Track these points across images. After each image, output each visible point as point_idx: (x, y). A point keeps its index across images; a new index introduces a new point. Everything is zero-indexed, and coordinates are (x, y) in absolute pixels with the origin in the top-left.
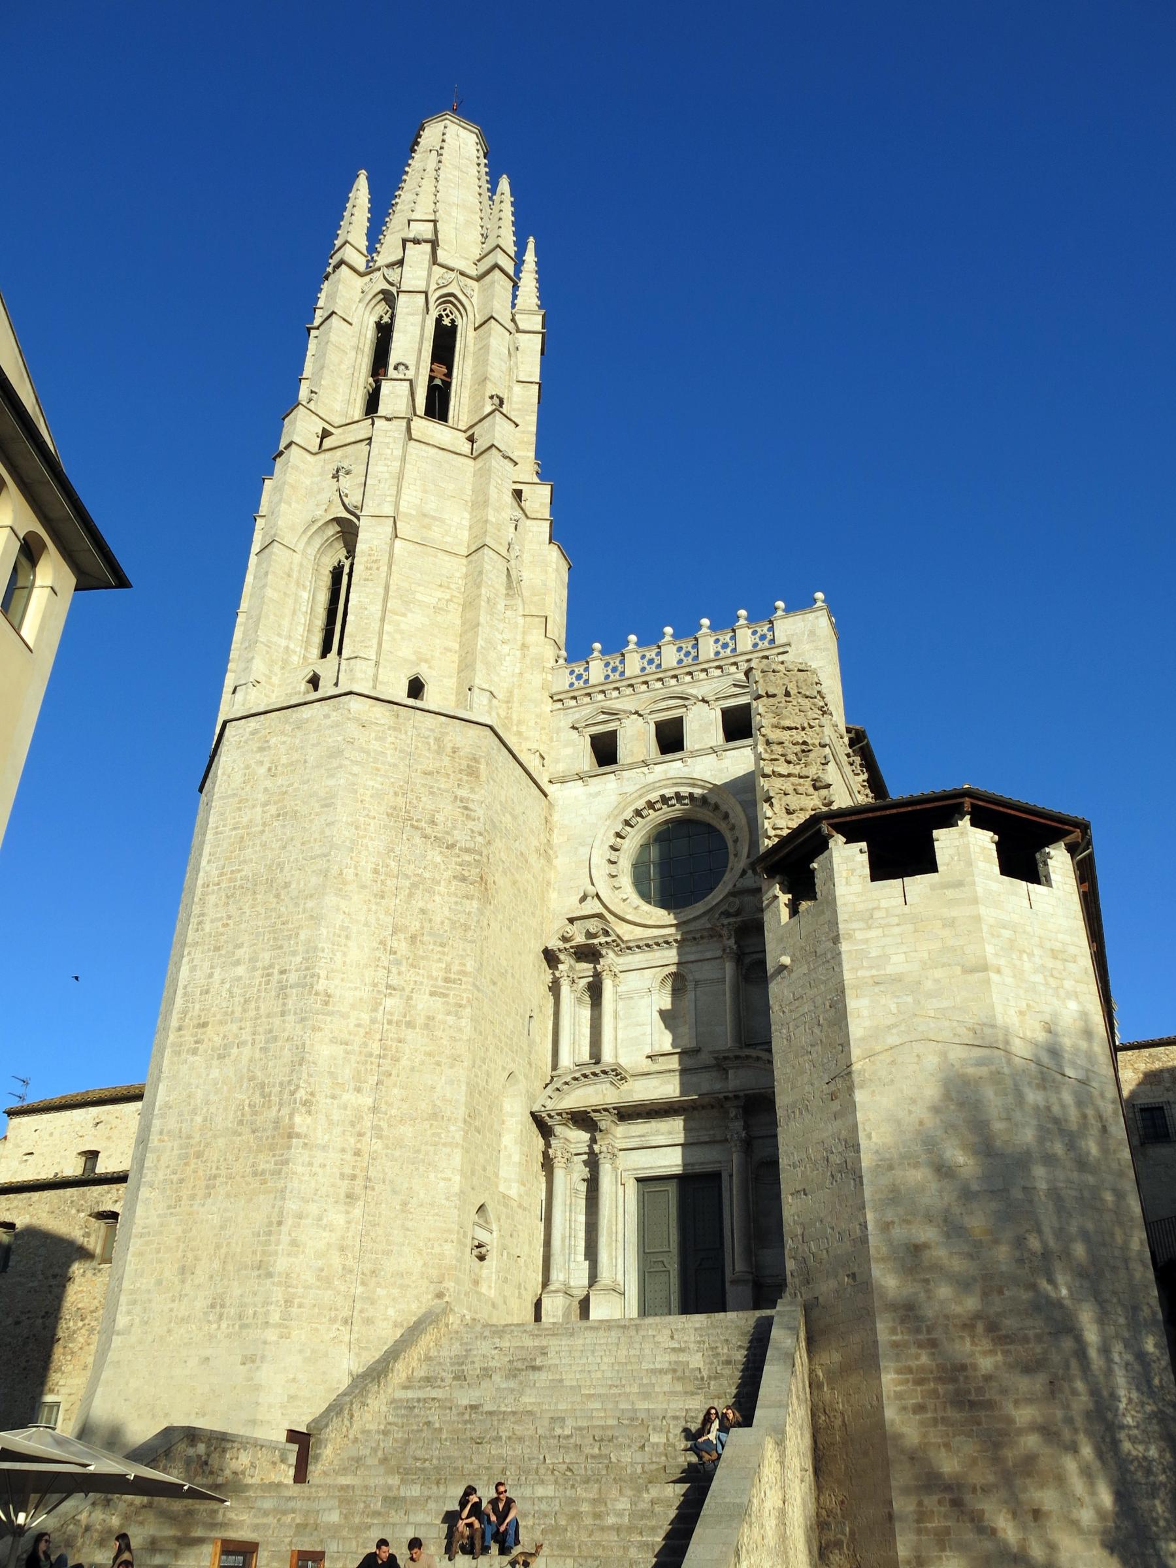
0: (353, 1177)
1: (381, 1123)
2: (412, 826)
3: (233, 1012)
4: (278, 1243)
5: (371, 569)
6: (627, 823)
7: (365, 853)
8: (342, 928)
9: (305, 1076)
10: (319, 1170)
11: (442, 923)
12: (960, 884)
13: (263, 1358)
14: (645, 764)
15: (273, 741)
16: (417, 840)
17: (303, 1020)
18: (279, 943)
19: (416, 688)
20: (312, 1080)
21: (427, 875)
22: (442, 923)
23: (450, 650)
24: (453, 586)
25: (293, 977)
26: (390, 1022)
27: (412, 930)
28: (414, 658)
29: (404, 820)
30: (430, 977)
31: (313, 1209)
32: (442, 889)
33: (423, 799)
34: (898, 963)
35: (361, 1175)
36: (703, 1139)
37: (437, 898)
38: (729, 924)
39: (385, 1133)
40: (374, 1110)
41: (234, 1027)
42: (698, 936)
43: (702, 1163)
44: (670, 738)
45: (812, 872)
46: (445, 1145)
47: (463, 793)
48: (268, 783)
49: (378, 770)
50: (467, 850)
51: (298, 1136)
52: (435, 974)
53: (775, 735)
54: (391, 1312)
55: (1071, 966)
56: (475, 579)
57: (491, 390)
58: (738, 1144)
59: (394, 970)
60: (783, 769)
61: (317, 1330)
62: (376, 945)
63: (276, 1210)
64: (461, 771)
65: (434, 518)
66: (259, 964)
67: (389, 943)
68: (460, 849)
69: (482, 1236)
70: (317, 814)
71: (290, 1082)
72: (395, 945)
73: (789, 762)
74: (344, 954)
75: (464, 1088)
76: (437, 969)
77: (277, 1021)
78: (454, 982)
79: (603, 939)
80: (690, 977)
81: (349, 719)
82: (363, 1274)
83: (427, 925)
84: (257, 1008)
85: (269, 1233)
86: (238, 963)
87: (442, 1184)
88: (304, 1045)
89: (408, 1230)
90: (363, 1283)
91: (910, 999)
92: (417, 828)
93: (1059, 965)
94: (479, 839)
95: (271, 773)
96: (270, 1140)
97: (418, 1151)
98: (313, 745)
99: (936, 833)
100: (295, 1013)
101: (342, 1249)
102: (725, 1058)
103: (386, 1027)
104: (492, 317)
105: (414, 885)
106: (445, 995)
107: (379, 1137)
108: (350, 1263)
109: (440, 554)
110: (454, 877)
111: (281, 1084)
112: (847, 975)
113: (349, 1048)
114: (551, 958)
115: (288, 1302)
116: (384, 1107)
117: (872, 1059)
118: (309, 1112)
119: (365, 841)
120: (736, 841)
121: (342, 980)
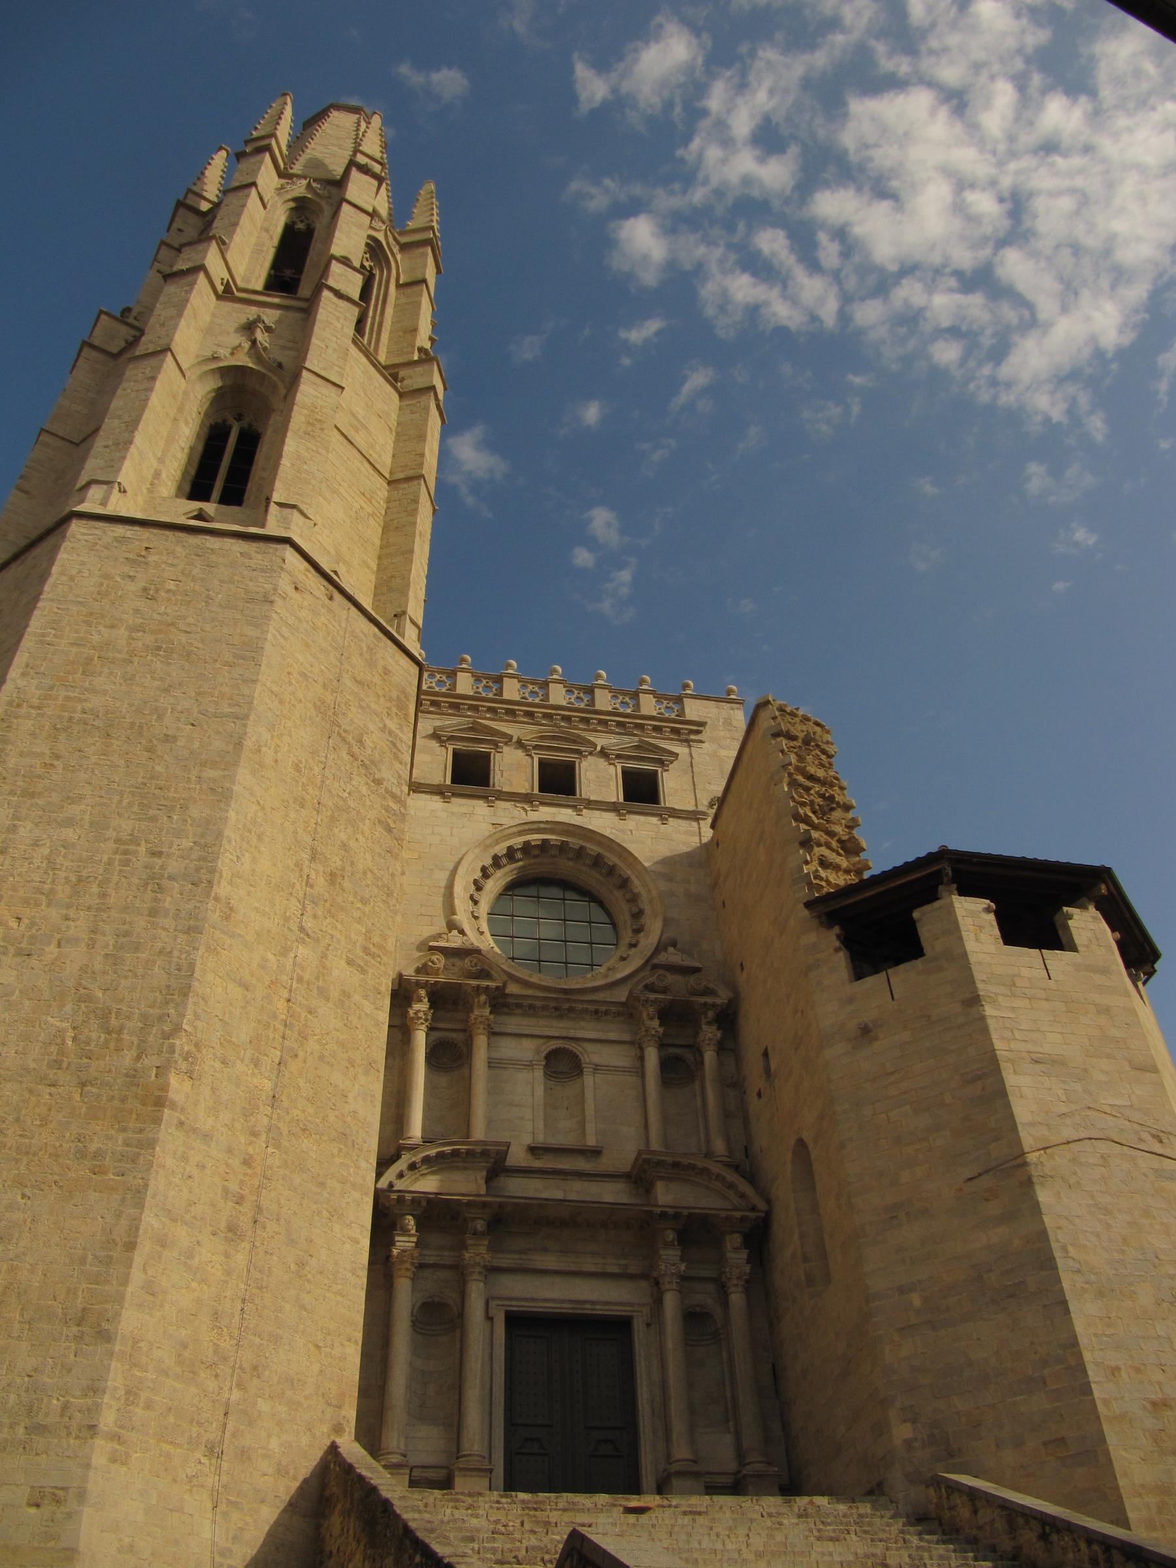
1: (280, 1125)
2: (339, 734)
3: (52, 891)
4: (125, 1280)
5: (313, 425)
6: (496, 858)
7: (286, 739)
10: (195, 1172)
13: (82, 1495)
15: (152, 558)
16: (344, 755)
17: (193, 930)
18: (151, 812)
20: (199, 1024)
21: (352, 804)
22: (365, 873)
23: (368, 567)
25: (174, 866)
26: (300, 980)
29: (330, 718)
34: (1052, 1043)
36: (610, 1269)
38: (655, 1001)
39: (285, 1143)
41: (54, 914)
42: (604, 1008)
43: (608, 1303)
44: (558, 781)
45: (912, 924)
48: (141, 604)
49: (307, 646)
51: (173, 1106)
52: (353, 936)
53: (800, 778)
54: (274, 1444)
58: (676, 1280)
61: (169, 1456)
63: (124, 1222)
64: (390, 700)
65: (362, 424)
66: (110, 833)
67: (306, 871)
68: (387, 791)
70: (226, 664)
71: (161, 1018)
72: (313, 875)
77: (141, 922)
78: (373, 956)
79: (485, 983)
80: (585, 1059)
81: (282, 568)
82: (241, 1368)
83: (348, 868)
84: (103, 895)
85: (108, 1261)
86: (69, 822)
88: (192, 966)
89: (303, 1307)
90: (240, 1386)
92: (344, 740)
95: (146, 594)
96: (116, 1103)
97: (322, 1185)
98: (222, 581)
100: (177, 916)
101: (216, 1316)
102: (659, 1163)
103: (295, 985)
106: (363, 971)
107: (278, 1146)
108: (226, 1344)
110: (379, 821)
111: (144, 1017)
112: (998, 1045)
113: (249, 996)
114: (401, 995)
115: (131, 1394)
116: (286, 1103)
117: (1048, 1151)
118: (190, 1075)
119: (289, 724)
120: (638, 915)
121: (249, 893)
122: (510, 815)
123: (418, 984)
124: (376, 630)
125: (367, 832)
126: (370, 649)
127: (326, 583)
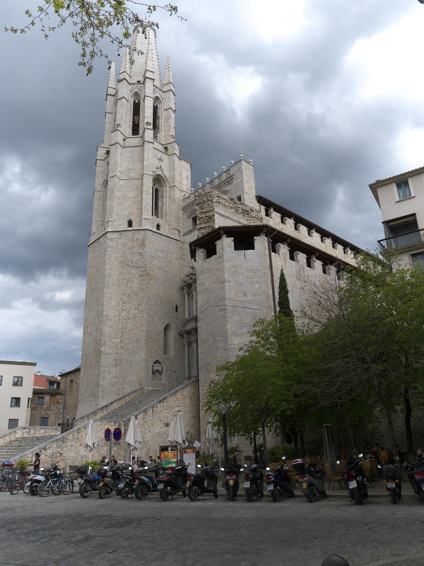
0: (117, 360)
8: (110, 297)
9: (103, 337)
11: (136, 289)
12: (220, 257)
16: (128, 268)
17: (102, 323)
19: (130, 224)
21: (131, 277)
22: (136, 289)
24: (138, 189)
26: (124, 319)
27: (128, 293)
28: (128, 214)
30: (134, 305)
31: (108, 369)
32: (136, 280)
33: (129, 256)
35: (119, 359)
37: (135, 283)
40: (121, 342)
41: (92, 327)
46: (140, 348)
47: (140, 251)
49: (116, 251)
50: (142, 267)
51: (102, 352)
52: (135, 304)
55: (258, 274)
59: (124, 305)
62: (118, 300)
65: (132, 169)
69: (155, 368)
72: (124, 298)
73: (205, 223)
74: (111, 304)
75: (145, 332)
76: (136, 302)
86: (92, 310)
87: (140, 358)
90: (121, 385)
91: (209, 294)
93: (254, 274)
94: (146, 263)
97: (133, 350)
101: (115, 377)
104: (145, 96)
105: (128, 281)
106: (138, 309)
107: (123, 349)
108: (118, 380)
109: (134, 180)
114: (182, 289)
118: (104, 346)
123: (184, 286)
124: (134, 231)
125: (136, 280)
126: (132, 238)
127: (118, 232)
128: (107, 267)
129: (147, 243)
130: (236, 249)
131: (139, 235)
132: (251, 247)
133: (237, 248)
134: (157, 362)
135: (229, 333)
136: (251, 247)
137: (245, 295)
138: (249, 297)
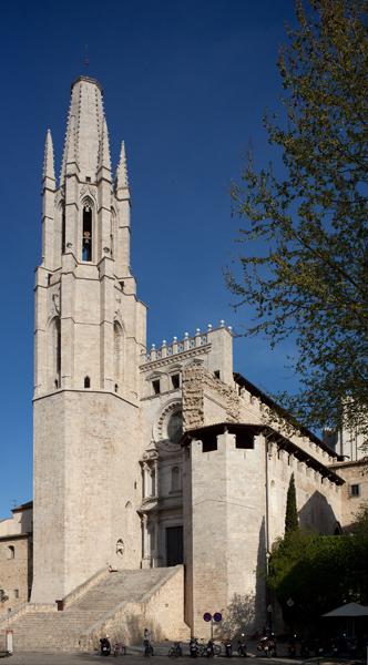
12: (222, 454)
14: (167, 393)
19: (87, 383)
34: (206, 478)
40: (86, 519)
53: (187, 396)
56: (102, 333)
57: (105, 245)
60: (189, 408)
69: (119, 547)
99: (218, 437)
114: (141, 464)
122: (165, 399)
128: (67, 434)
129: (110, 410)
130: (237, 447)
131: (102, 399)
132: (251, 447)
133: (238, 446)
134: (120, 541)
135: (229, 528)
136: (251, 446)
137: (244, 494)
138: (247, 497)
